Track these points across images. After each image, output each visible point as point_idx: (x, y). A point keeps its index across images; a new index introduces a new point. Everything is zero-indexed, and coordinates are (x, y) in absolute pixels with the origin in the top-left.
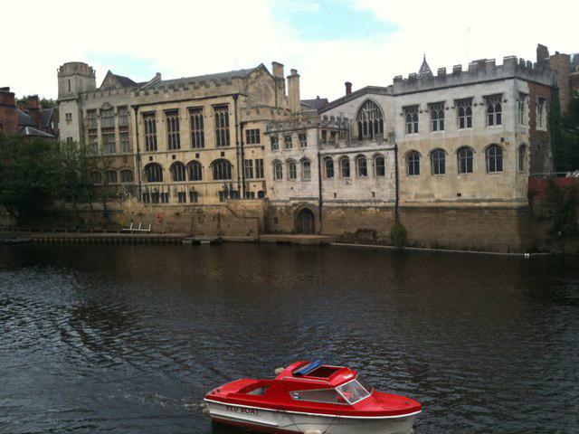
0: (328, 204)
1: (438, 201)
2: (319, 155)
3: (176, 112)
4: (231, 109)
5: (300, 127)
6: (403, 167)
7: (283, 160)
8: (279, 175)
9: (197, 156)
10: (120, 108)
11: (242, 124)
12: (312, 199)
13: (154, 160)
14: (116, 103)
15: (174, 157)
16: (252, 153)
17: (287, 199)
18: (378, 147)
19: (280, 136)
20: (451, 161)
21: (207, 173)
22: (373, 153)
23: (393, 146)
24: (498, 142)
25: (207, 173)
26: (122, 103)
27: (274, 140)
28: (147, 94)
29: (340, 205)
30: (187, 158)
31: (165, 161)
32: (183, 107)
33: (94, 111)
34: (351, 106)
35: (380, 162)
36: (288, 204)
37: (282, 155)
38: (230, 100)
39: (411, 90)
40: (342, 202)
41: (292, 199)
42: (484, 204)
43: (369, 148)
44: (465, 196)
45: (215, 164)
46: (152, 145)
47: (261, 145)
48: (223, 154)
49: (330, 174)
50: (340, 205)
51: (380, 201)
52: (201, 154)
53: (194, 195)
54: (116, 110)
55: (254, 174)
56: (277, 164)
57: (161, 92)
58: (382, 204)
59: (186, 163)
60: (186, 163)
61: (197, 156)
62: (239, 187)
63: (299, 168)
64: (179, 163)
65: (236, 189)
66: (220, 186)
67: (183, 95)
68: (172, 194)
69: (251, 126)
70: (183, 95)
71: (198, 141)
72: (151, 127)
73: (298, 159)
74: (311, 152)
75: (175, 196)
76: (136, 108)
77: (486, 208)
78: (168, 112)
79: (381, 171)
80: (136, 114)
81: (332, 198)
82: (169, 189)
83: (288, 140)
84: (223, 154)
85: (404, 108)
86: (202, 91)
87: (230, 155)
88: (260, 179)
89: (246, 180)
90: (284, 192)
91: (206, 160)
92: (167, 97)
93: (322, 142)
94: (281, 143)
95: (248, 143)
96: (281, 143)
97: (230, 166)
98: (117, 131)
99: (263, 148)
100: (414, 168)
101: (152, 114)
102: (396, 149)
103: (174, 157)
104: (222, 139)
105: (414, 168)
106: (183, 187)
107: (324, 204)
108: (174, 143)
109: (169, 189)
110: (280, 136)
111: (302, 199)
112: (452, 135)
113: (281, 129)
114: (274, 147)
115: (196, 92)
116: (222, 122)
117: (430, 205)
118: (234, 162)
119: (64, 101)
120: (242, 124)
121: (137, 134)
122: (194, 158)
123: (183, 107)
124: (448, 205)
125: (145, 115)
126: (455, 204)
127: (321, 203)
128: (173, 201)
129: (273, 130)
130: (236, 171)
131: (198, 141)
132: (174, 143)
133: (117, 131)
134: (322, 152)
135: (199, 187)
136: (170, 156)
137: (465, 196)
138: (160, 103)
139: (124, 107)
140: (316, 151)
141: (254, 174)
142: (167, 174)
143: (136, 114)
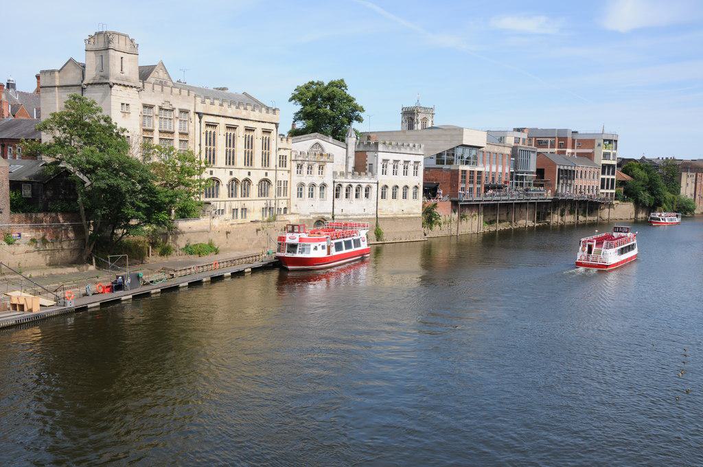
0: (339, 217)
1: (395, 214)
2: (334, 182)
3: (234, 128)
4: (274, 134)
5: (322, 160)
6: (380, 194)
7: (307, 183)
8: (300, 195)
9: (249, 174)
10: (182, 111)
11: (280, 149)
12: (328, 213)
13: (214, 175)
14: (179, 104)
15: (231, 173)
16: (283, 176)
17: (308, 213)
18: (369, 181)
19: (305, 165)
20: (400, 192)
21: (254, 190)
22: (367, 184)
23: (376, 182)
24: (417, 185)
25: (254, 190)
26: (185, 107)
27: (300, 167)
28: (212, 104)
29: (346, 217)
30: (241, 175)
31: (224, 177)
32: (242, 124)
33: (151, 107)
34: (306, 145)
35: (367, 190)
36: (309, 218)
37: (307, 179)
38: (273, 127)
39: (385, 150)
40: (347, 215)
41: (311, 214)
42: (412, 215)
43: (365, 180)
44: (405, 211)
45: (261, 181)
46: (211, 159)
47: (288, 168)
48: (266, 174)
49: (337, 196)
50: (346, 217)
51: (368, 214)
52: (252, 171)
53: (244, 210)
54: (177, 113)
55: (282, 194)
56: (301, 186)
57: (225, 105)
58: (369, 216)
59: (241, 180)
60: (241, 180)
61: (249, 174)
62: (275, 204)
63: (317, 191)
64: (235, 180)
65: (274, 206)
66: (262, 204)
67: (243, 113)
68: (227, 210)
69: (282, 153)
70: (243, 113)
71: (249, 160)
72: (211, 140)
73: (318, 183)
74: (328, 180)
75: (230, 213)
76: (200, 115)
77: (412, 218)
78: (229, 127)
79: (367, 196)
80: (200, 122)
81: (340, 213)
82: (225, 205)
83: (310, 168)
84: (266, 174)
85: (384, 160)
86: (255, 115)
87: (271, 176)
88: (285, 197)
89: (277, 198)
90: (306, 208)
91: (256, 176)
92: (231, 111)
93: (335, 173)
94: (305, 169)
95: (280, 166)
96: (305, 169)
97: (269, 182)
98: (177, 137)
99: (289, 171)
100: (383, 196)
101: (214, 125)
102: (378, 183)
103: (231, 173)
104: (266, 161)
105: (383, 196)
106: (237, 203)
107: (335, 217)
108: (230, 159)
109: (225, 205)
110: (305, 165)
111: (321, 214)
112: (401, 180)
113: (307, 159)
114: (299, 173)
115: (252, 113)
116: (266, 145)
117: (391, 216)
118: (273, 181)
119: (120, 85)
120: (280, 149)
121: (200, 145)
122: (247, 176)
123: (259, 127)
124: (398, 216)
125: (208, 125)
126: (401, 216)
127: (333, 217)
128: (228, 215)
129: (300, 158)
130: (273, 190)
131: (249, 160)
132: (230, 159)
133: (177, 137)
134: (336, 180)
135: (248, 205)
136: (228, 171)
137: (405, 211)
138: (223, 116)
139: (186, 112)
140: (332, 180)
141: (282, 194)
142: (223, 190)
143: (200, 122)
